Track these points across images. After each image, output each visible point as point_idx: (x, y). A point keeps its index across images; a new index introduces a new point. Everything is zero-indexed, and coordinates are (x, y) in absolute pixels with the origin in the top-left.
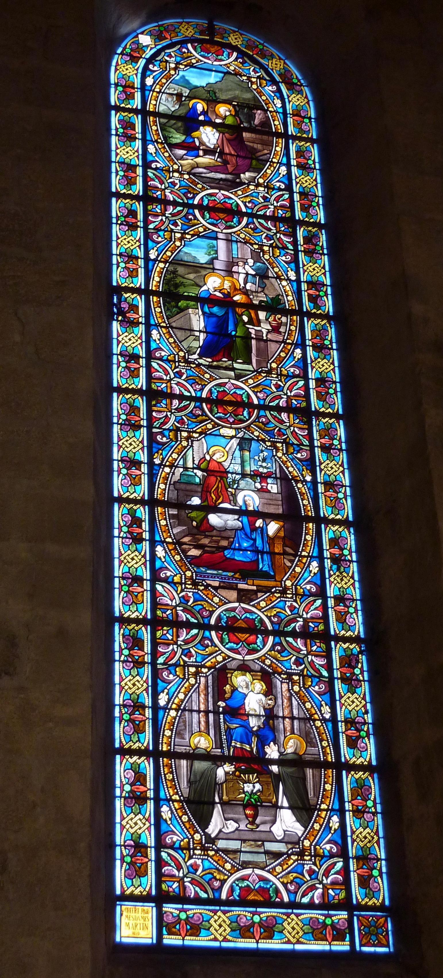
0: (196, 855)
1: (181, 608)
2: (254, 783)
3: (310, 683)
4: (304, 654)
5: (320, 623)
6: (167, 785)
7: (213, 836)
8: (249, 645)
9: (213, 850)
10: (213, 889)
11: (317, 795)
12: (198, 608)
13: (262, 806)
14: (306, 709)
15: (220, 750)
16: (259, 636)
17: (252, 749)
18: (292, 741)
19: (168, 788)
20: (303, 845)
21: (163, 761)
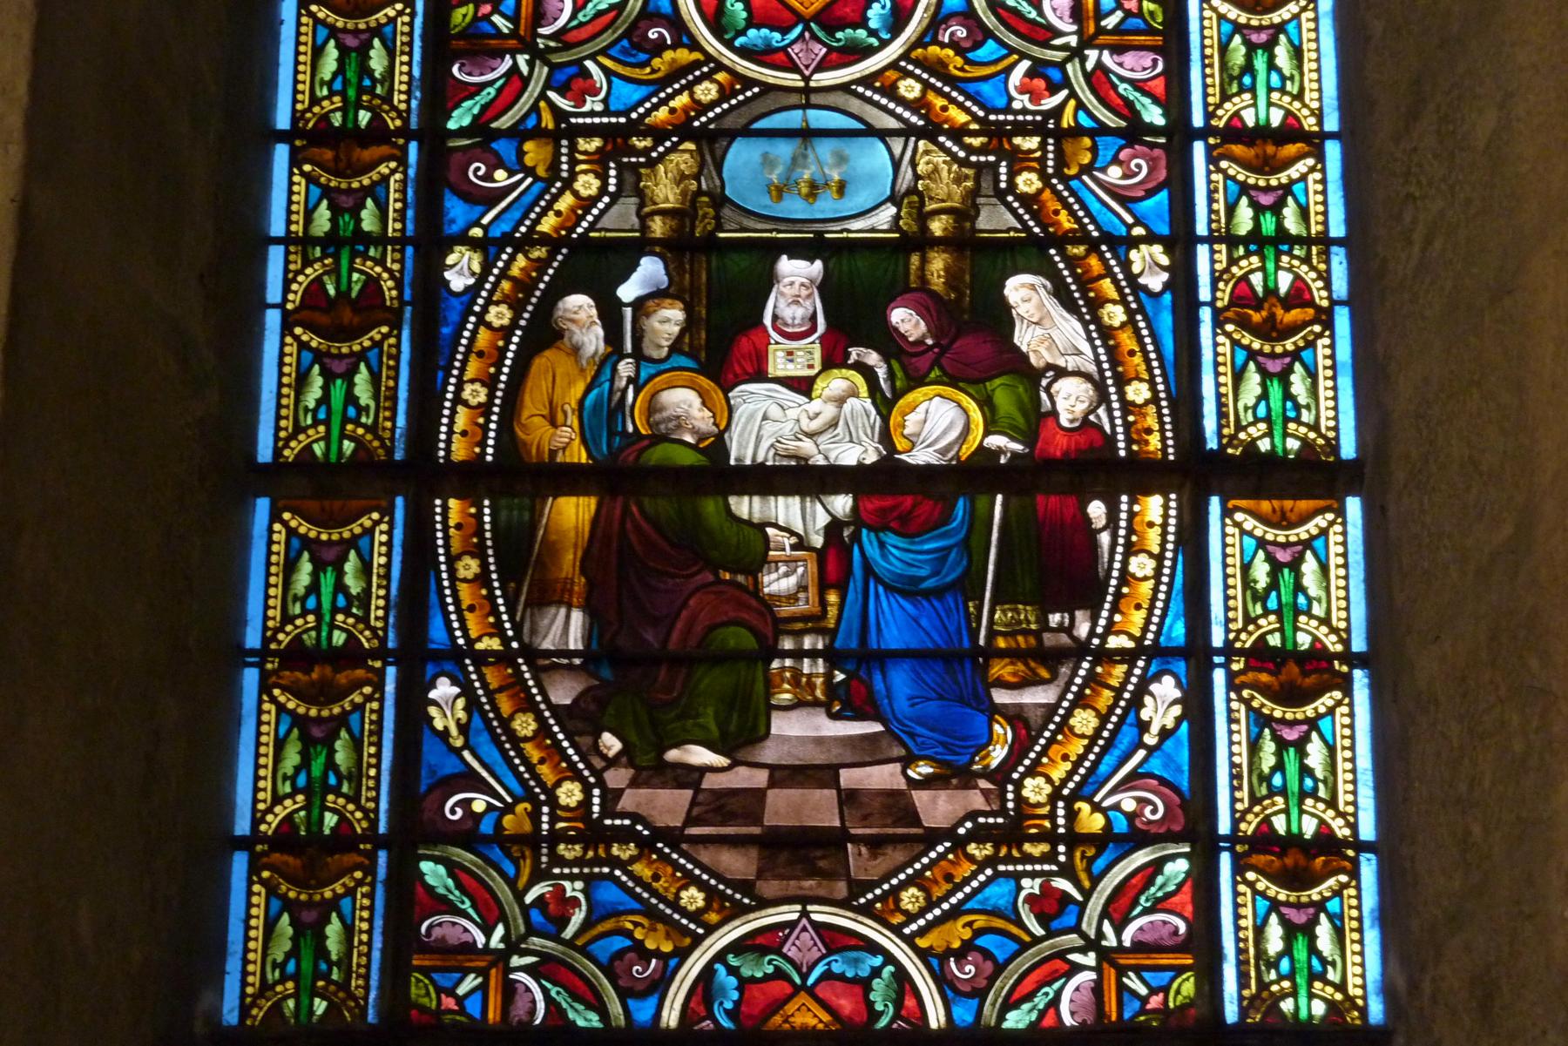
0: (562, 862)
3: (1086, 159)
10: (623, 995)
21: (445, 508)
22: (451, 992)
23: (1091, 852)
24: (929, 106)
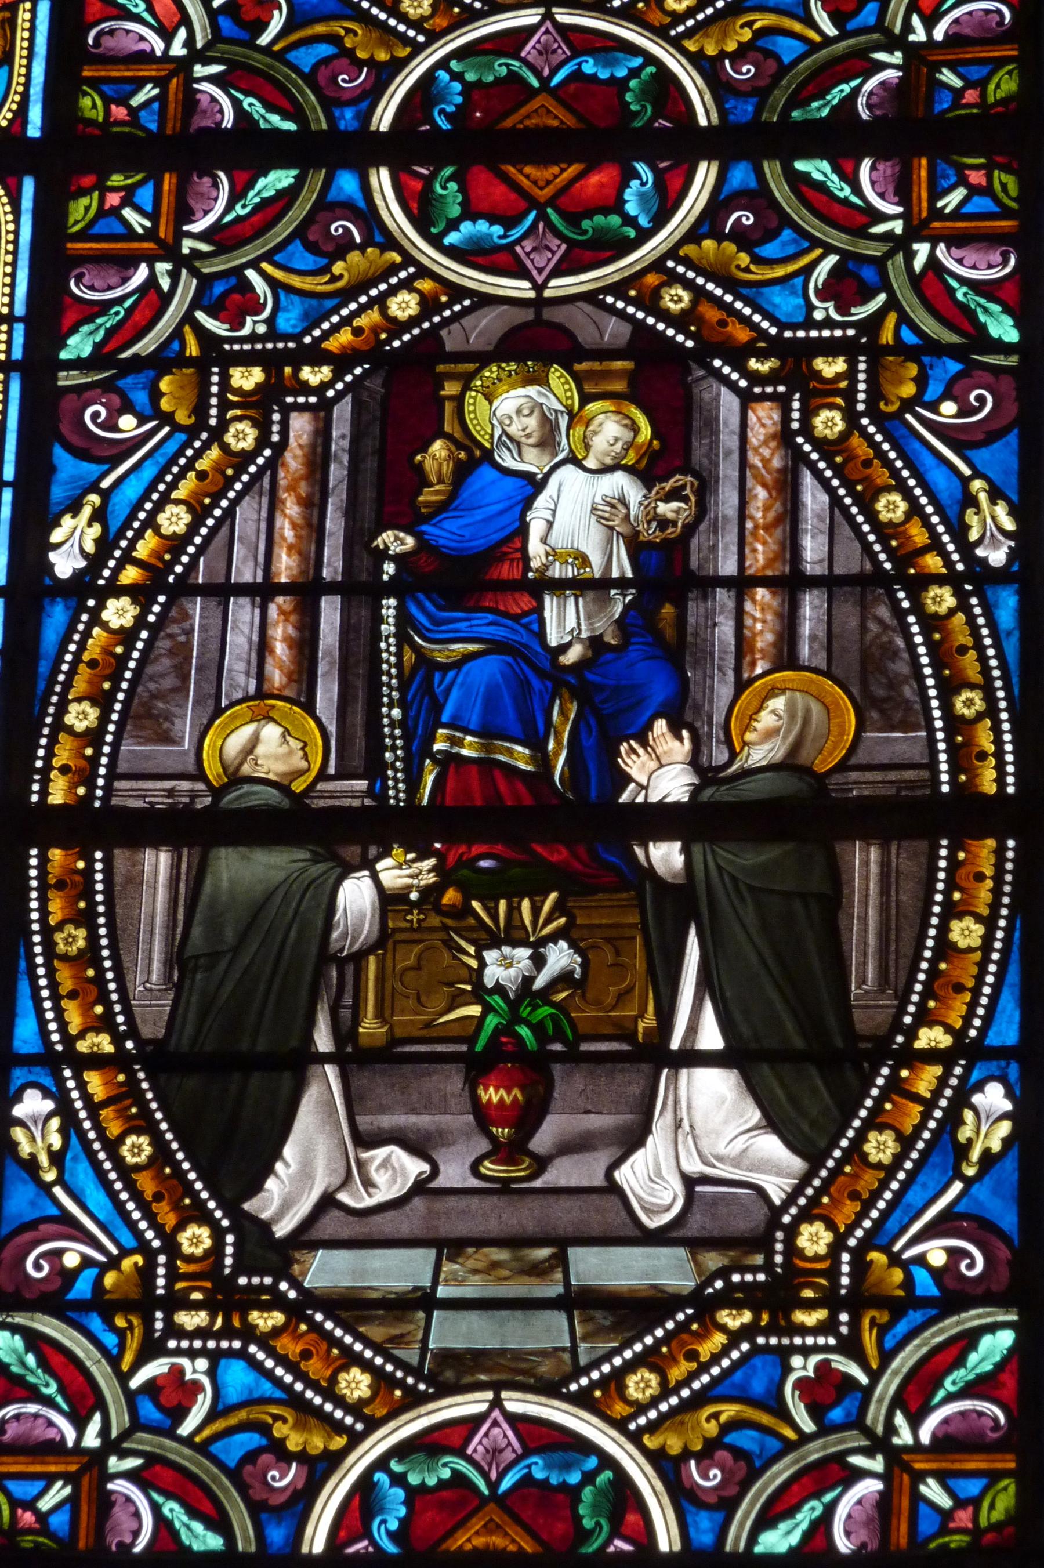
0: (180, 1333)
1: (216, 69)
2: (543, 942)
3: (909, 390)
4: (888, 236)
5: (999, 63)
6: (53, 985)
7: (282, 1230)
8: (573, 219)
9: (278, 1302)
10: (257, 1509)
11: (895, 982)
12: (306, 58)
13: (573, 1057)
14: (878, 526)
15: (362, 785)
16: (641, 168)
17: (544, 762)
18: (778, 703)
19: (56, 997)
20: (792, 1250)
22: (30, 1505)
23: (884, 1317)
24: (700, 321)
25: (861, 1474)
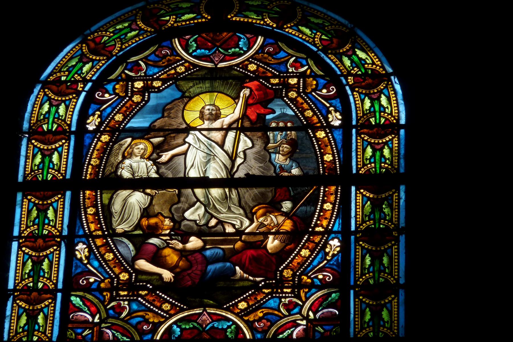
0: (120, 296)
25: (300, 325)
